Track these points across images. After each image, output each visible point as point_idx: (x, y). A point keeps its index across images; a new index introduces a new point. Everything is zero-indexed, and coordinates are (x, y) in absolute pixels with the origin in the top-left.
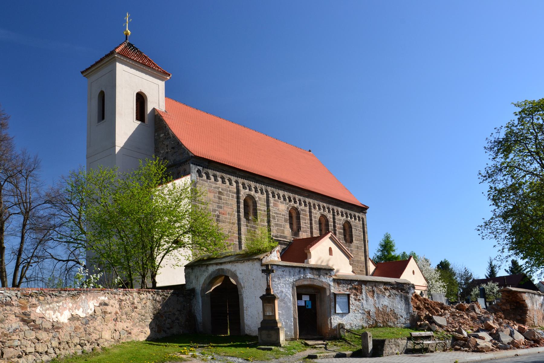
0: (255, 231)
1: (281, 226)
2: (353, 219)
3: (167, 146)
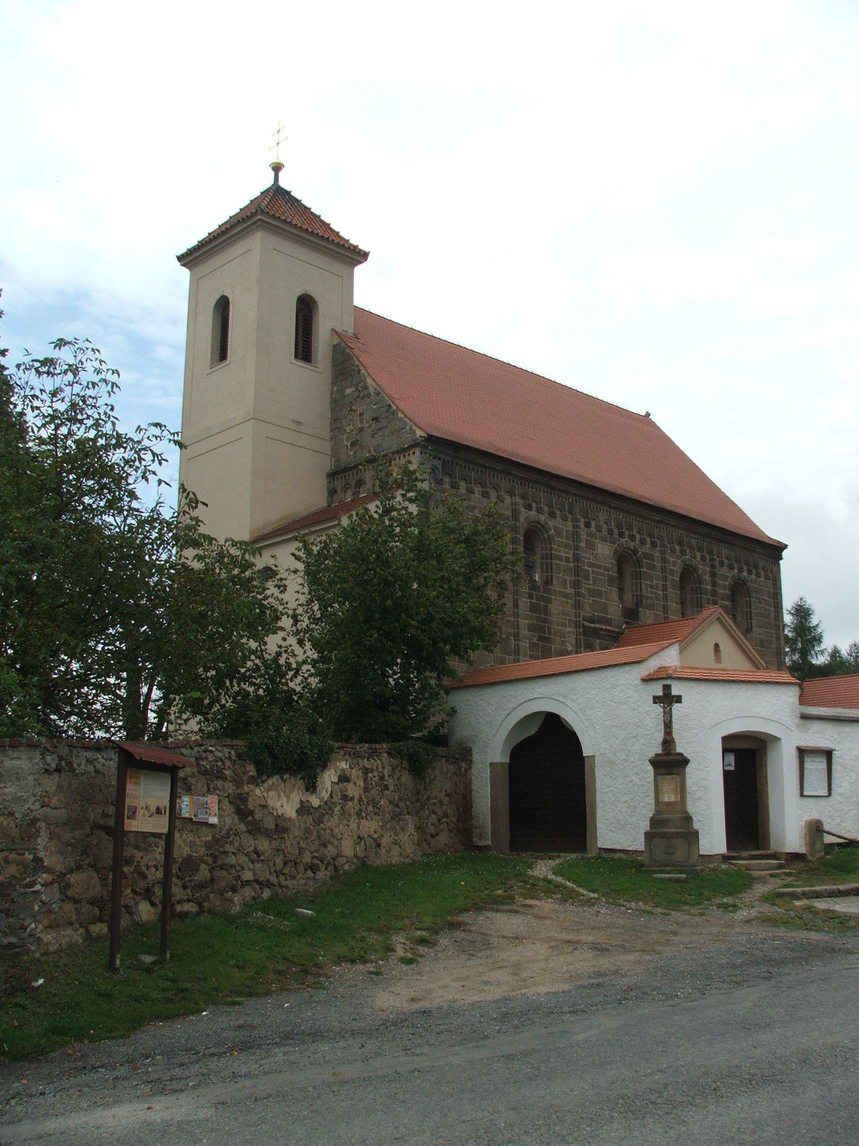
0: (546, 607)
1: (598, 594)
2: (753, 576)
3: (361, 415)
